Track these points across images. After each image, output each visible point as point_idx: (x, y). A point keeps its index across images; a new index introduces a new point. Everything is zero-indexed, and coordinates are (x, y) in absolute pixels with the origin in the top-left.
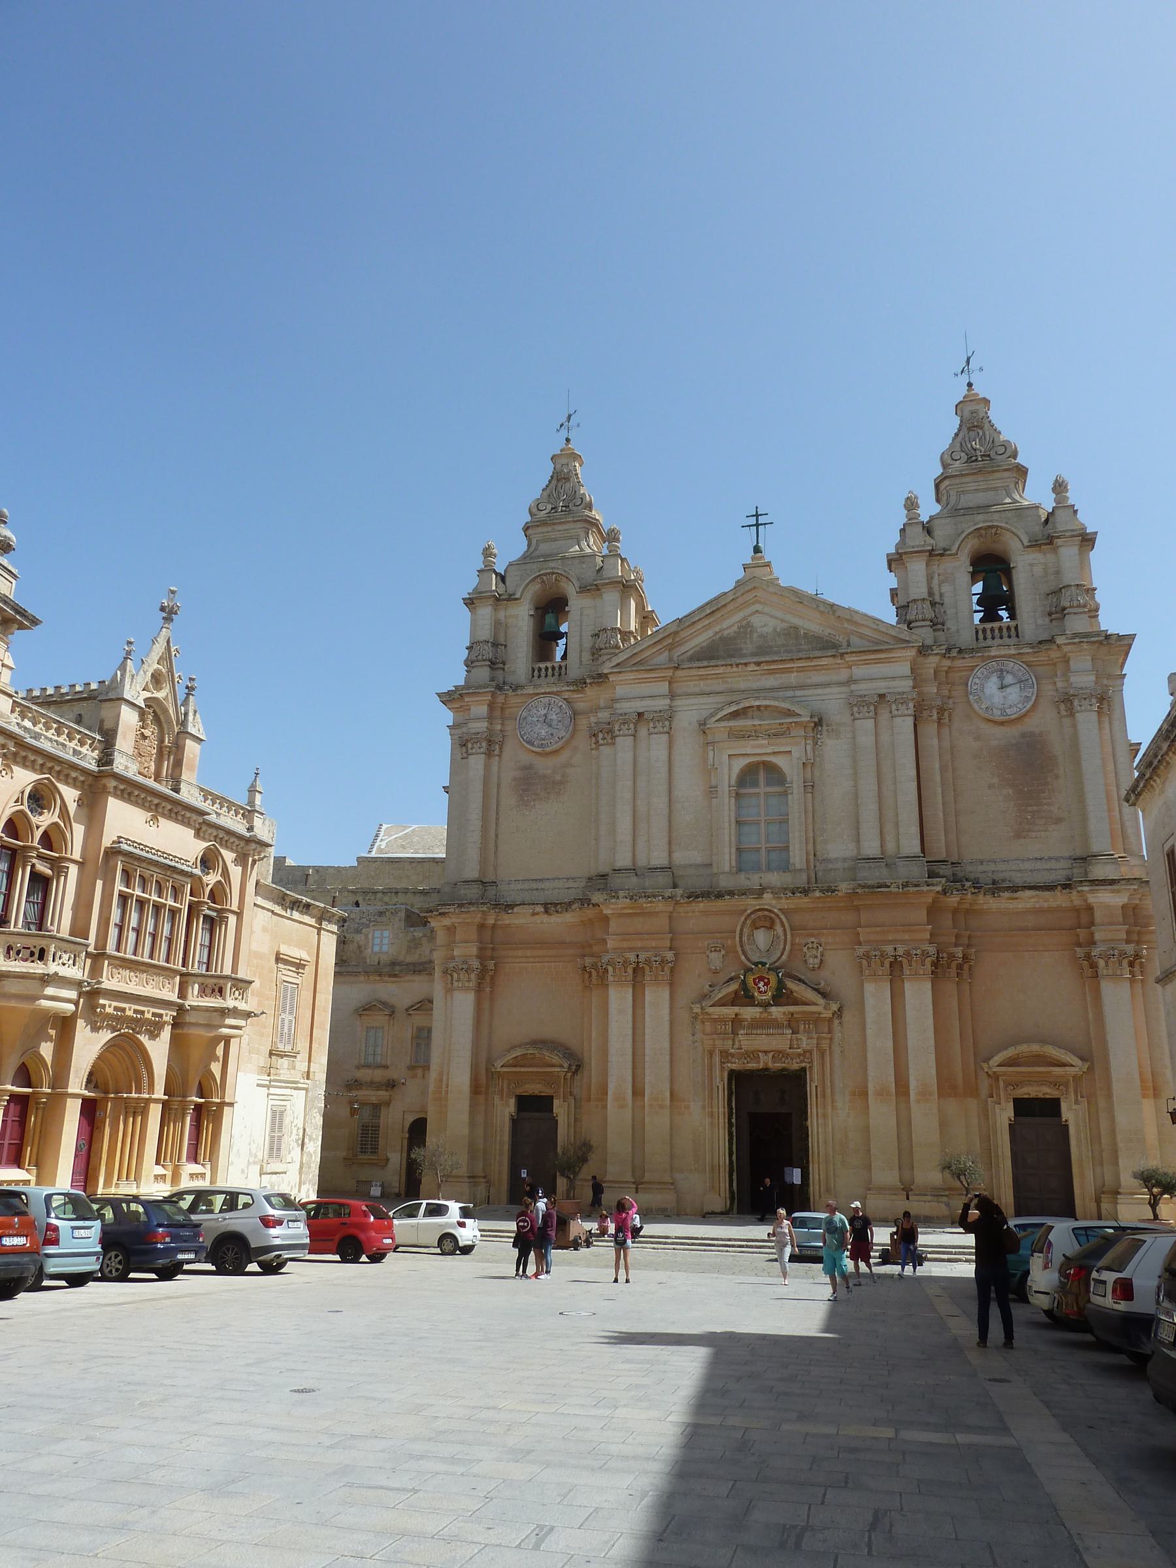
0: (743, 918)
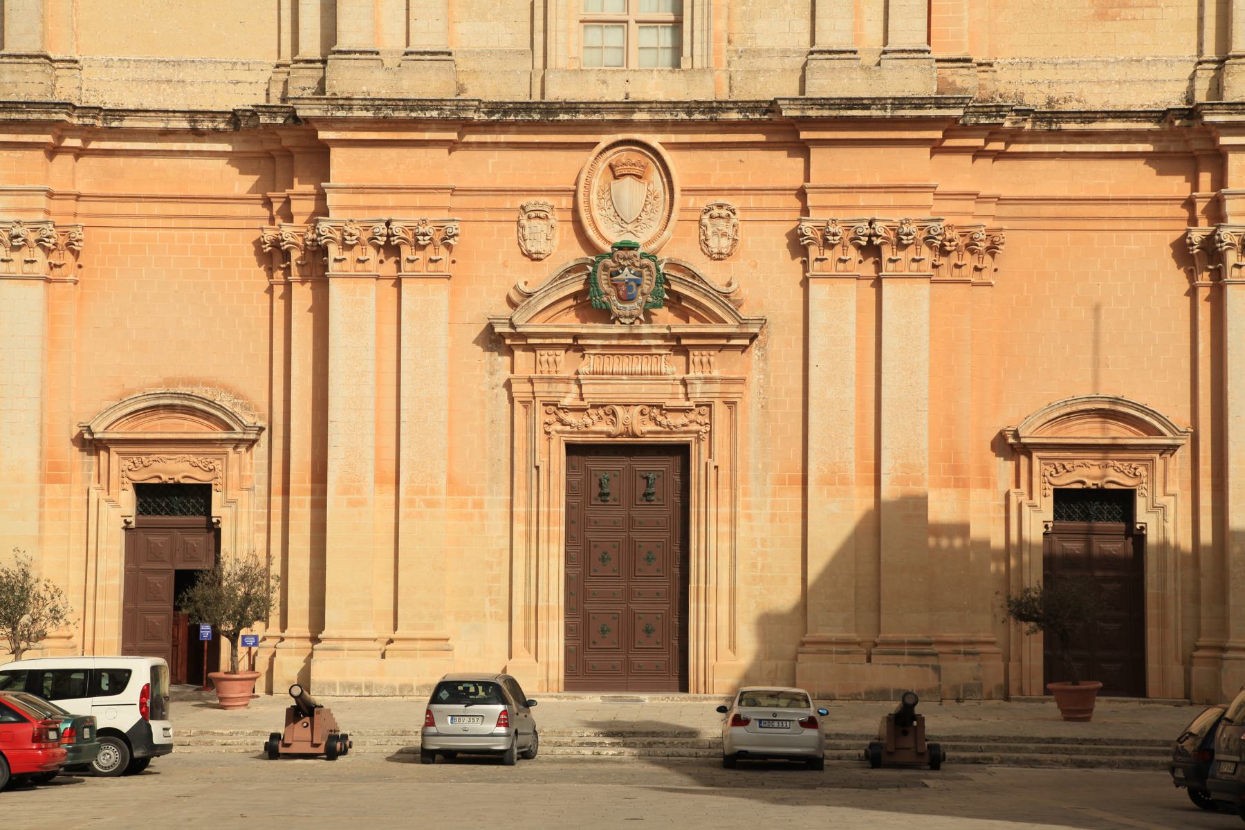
0: (592, 158)
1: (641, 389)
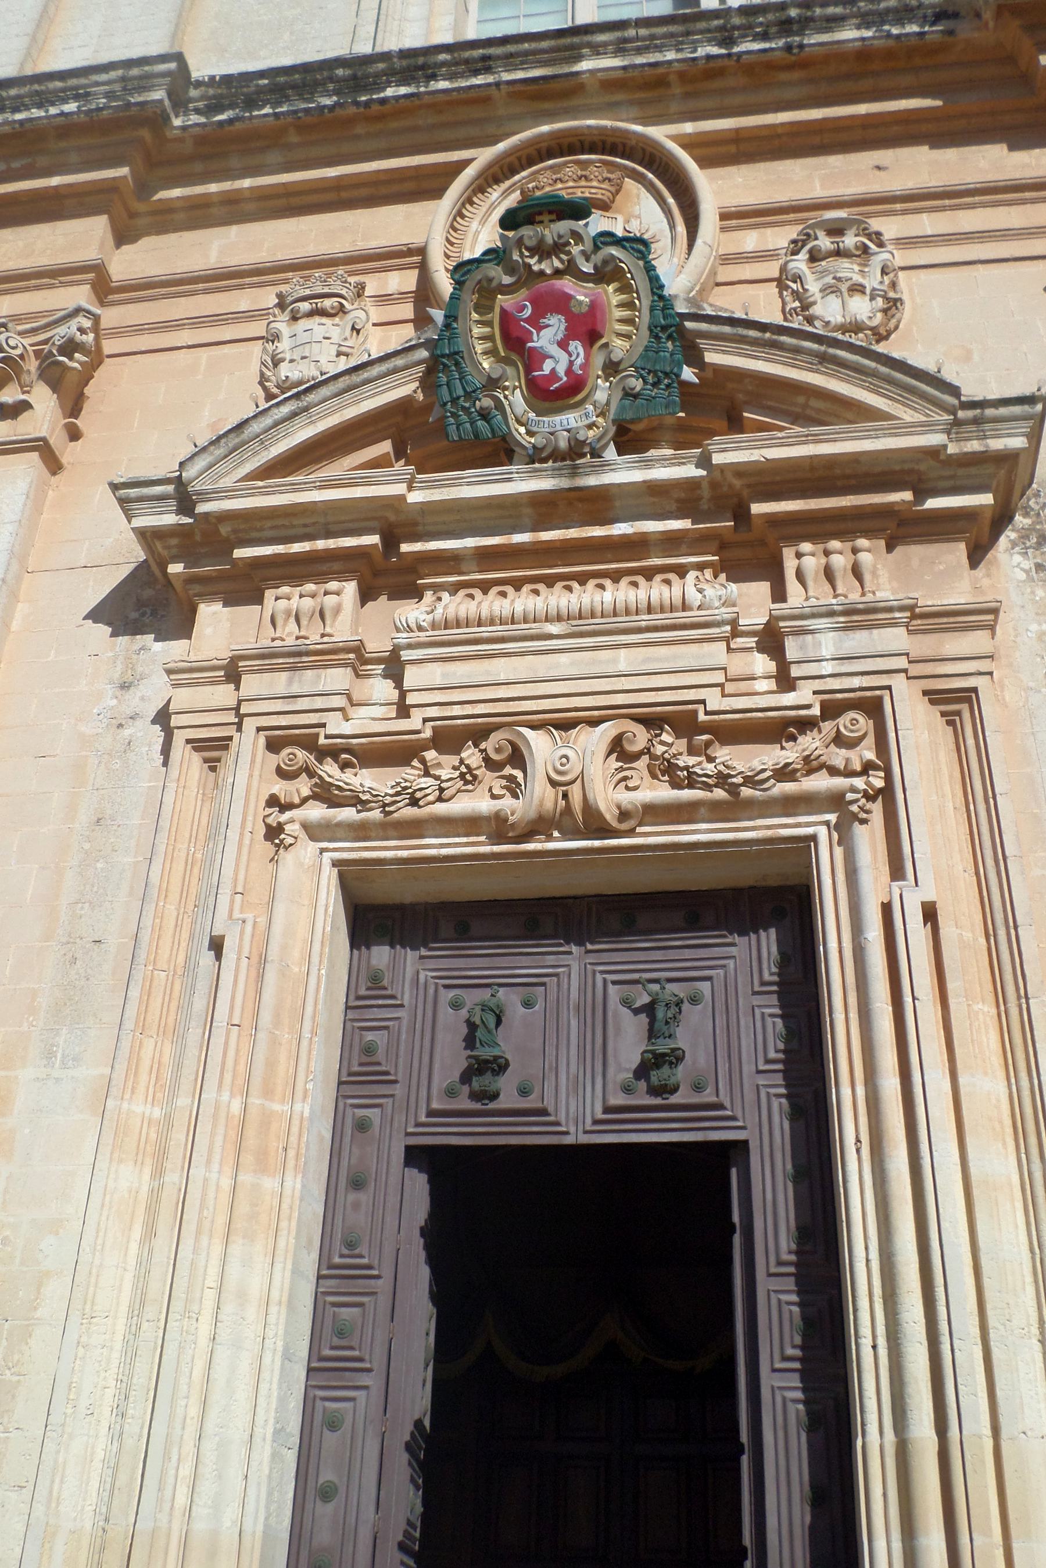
1: (615, 661)
